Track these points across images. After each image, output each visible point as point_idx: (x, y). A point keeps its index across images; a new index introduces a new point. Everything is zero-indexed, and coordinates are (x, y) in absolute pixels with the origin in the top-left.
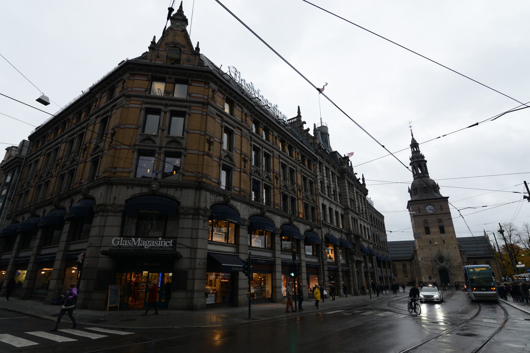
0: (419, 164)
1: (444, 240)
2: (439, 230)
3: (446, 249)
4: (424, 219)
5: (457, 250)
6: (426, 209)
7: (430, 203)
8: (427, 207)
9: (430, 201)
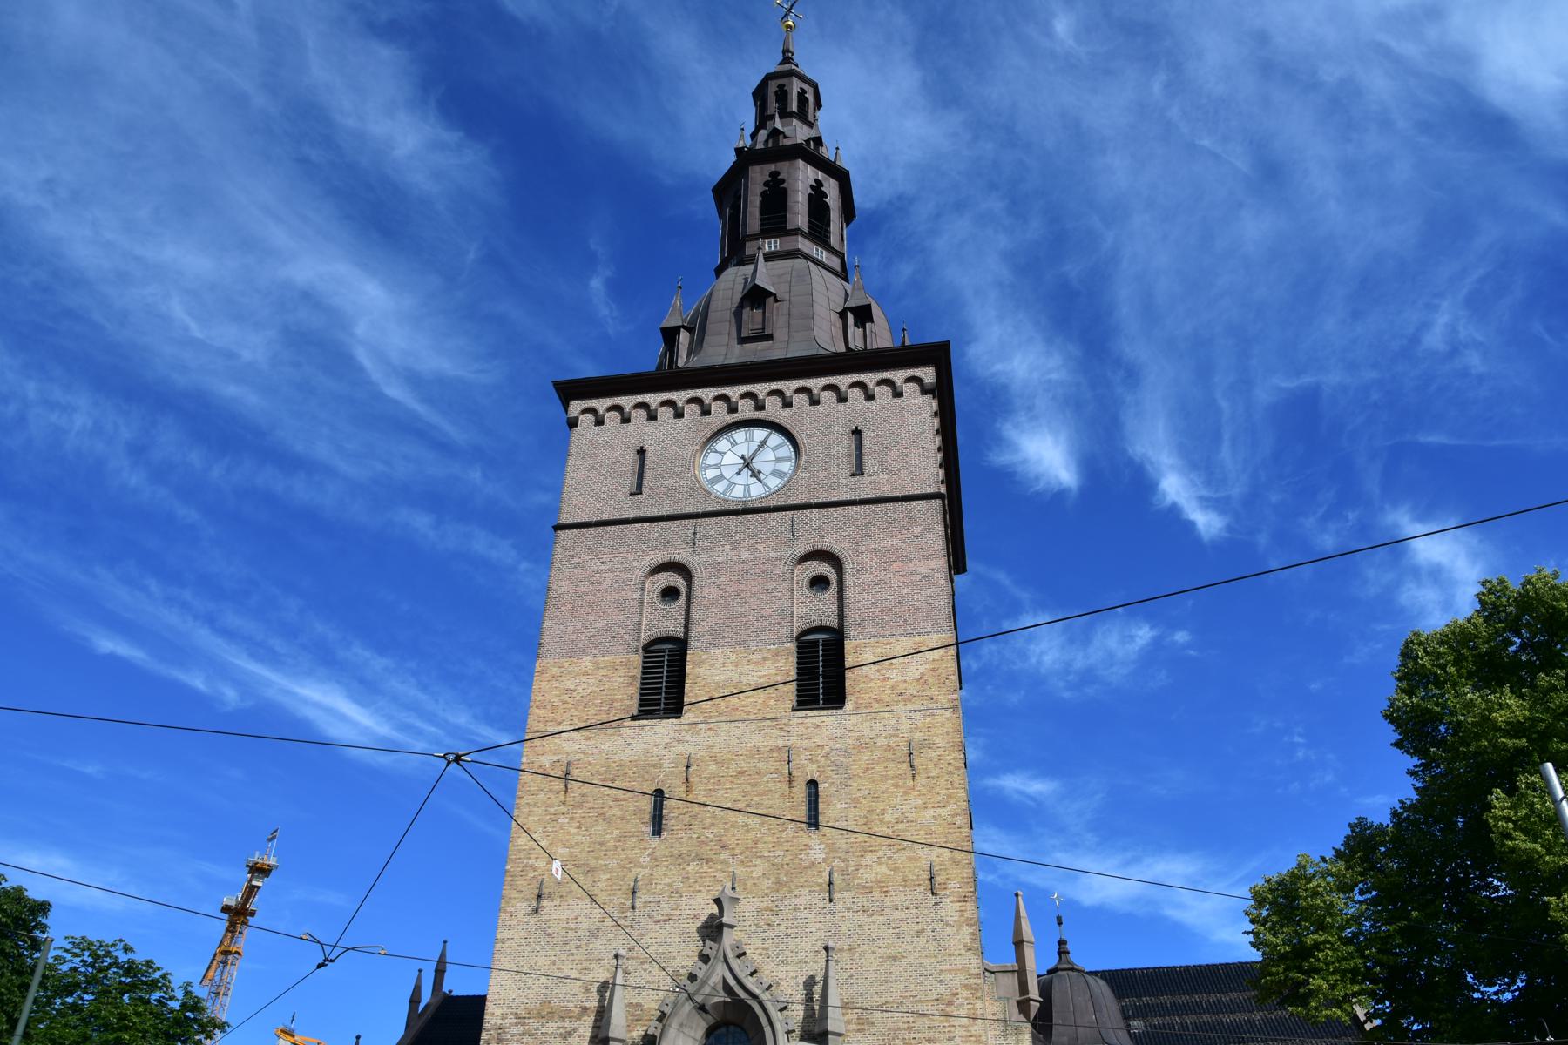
0: (774, 174)
1: (813, 784)
2: (787, 666)
3: (820, 899)
4: (659, 557)
5: (950, 909)
6: (712, 459)
7: (760, 407)
8: (722, 444)
9: (761, 389)
